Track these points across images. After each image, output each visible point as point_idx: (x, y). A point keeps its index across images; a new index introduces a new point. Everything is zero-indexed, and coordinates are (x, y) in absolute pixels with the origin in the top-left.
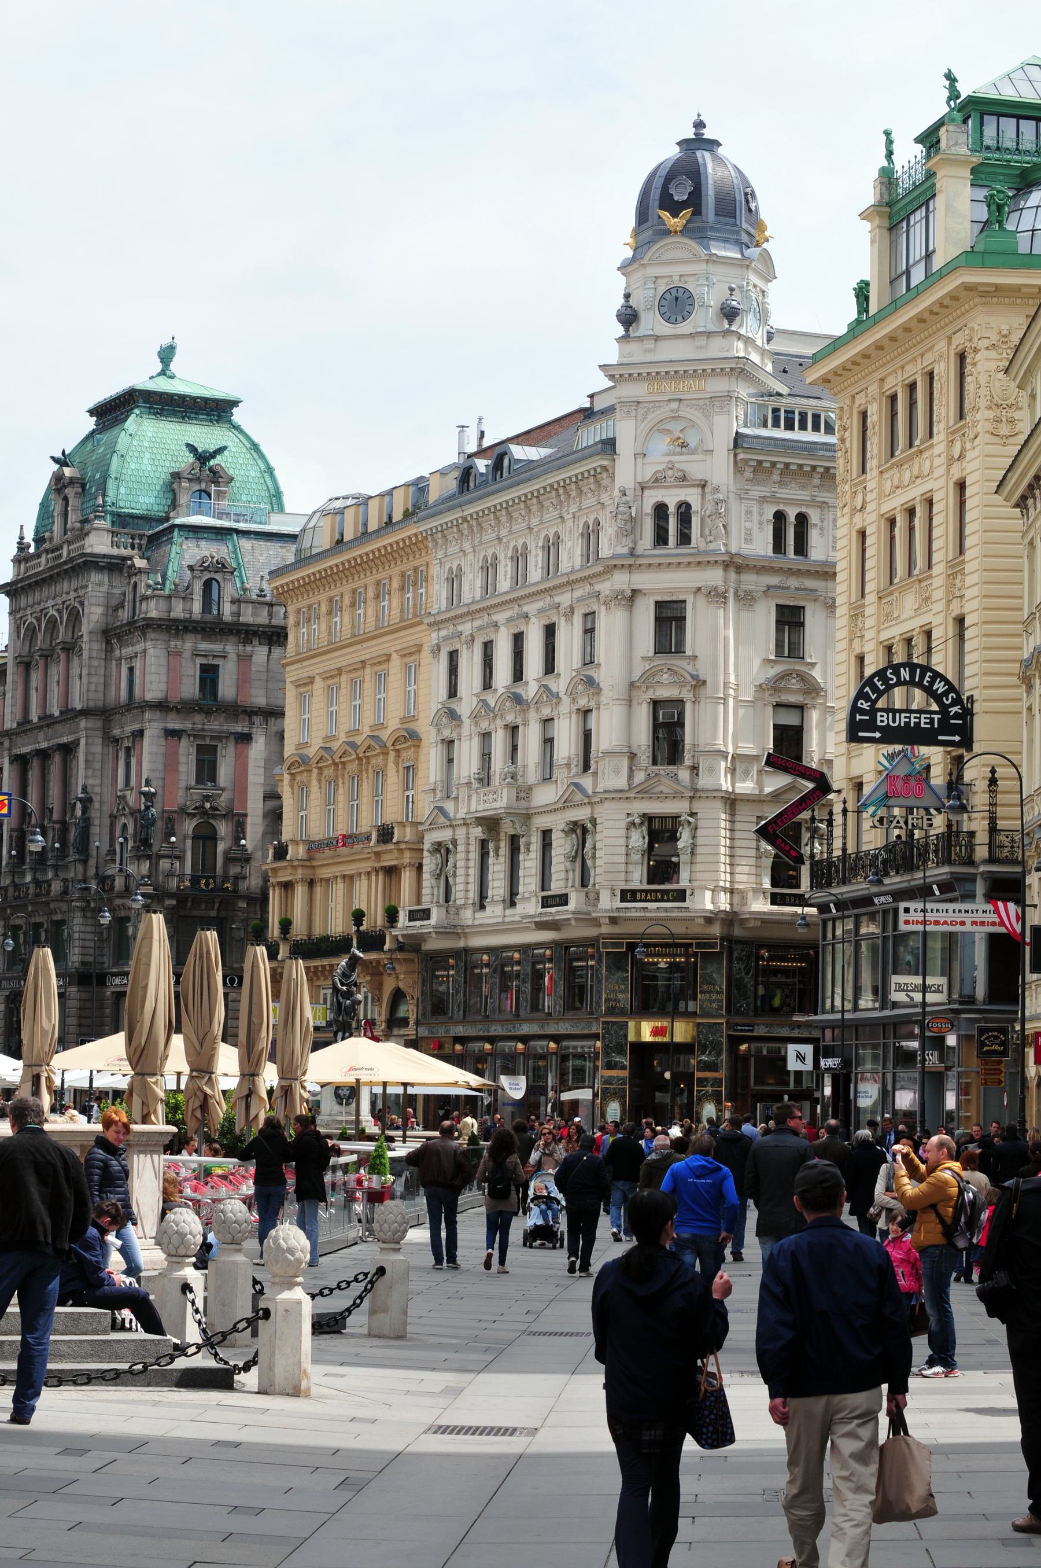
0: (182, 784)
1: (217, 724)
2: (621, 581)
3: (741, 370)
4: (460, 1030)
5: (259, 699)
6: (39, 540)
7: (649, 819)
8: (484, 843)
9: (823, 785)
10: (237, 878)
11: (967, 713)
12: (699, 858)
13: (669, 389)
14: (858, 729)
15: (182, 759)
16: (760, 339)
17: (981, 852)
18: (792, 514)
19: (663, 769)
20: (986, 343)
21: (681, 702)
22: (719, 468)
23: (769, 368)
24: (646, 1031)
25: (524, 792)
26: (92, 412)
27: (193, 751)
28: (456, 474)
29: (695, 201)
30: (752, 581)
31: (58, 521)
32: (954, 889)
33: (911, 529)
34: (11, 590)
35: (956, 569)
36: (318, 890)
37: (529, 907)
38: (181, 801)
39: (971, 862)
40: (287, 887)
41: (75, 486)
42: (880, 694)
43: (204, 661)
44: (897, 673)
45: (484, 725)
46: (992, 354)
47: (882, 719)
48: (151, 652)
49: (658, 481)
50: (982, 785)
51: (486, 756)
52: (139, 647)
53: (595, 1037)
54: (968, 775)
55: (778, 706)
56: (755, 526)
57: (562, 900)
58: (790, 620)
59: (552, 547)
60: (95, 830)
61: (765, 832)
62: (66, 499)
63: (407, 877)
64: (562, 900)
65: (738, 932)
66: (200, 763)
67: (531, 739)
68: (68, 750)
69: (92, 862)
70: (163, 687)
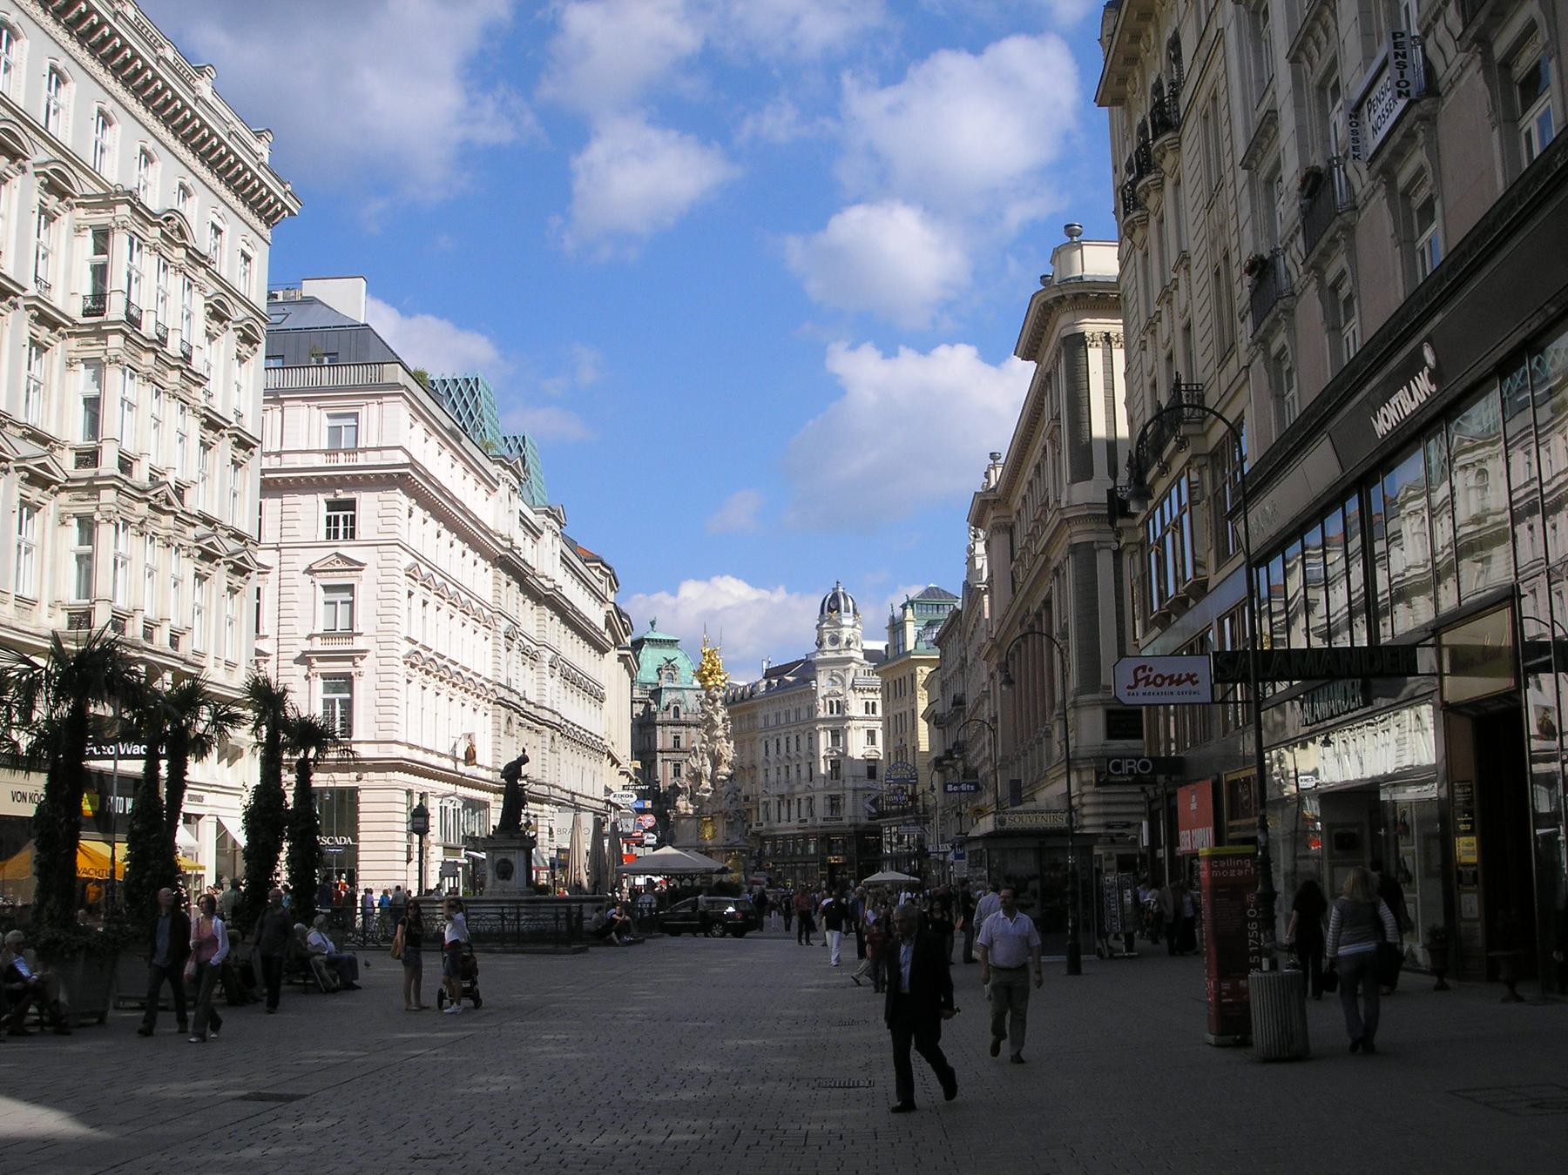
1: (679, 756)
3: (850, 660)
37: (794, 823)
49: (829, 695)
59: (798, 711)
67: (793, 770)
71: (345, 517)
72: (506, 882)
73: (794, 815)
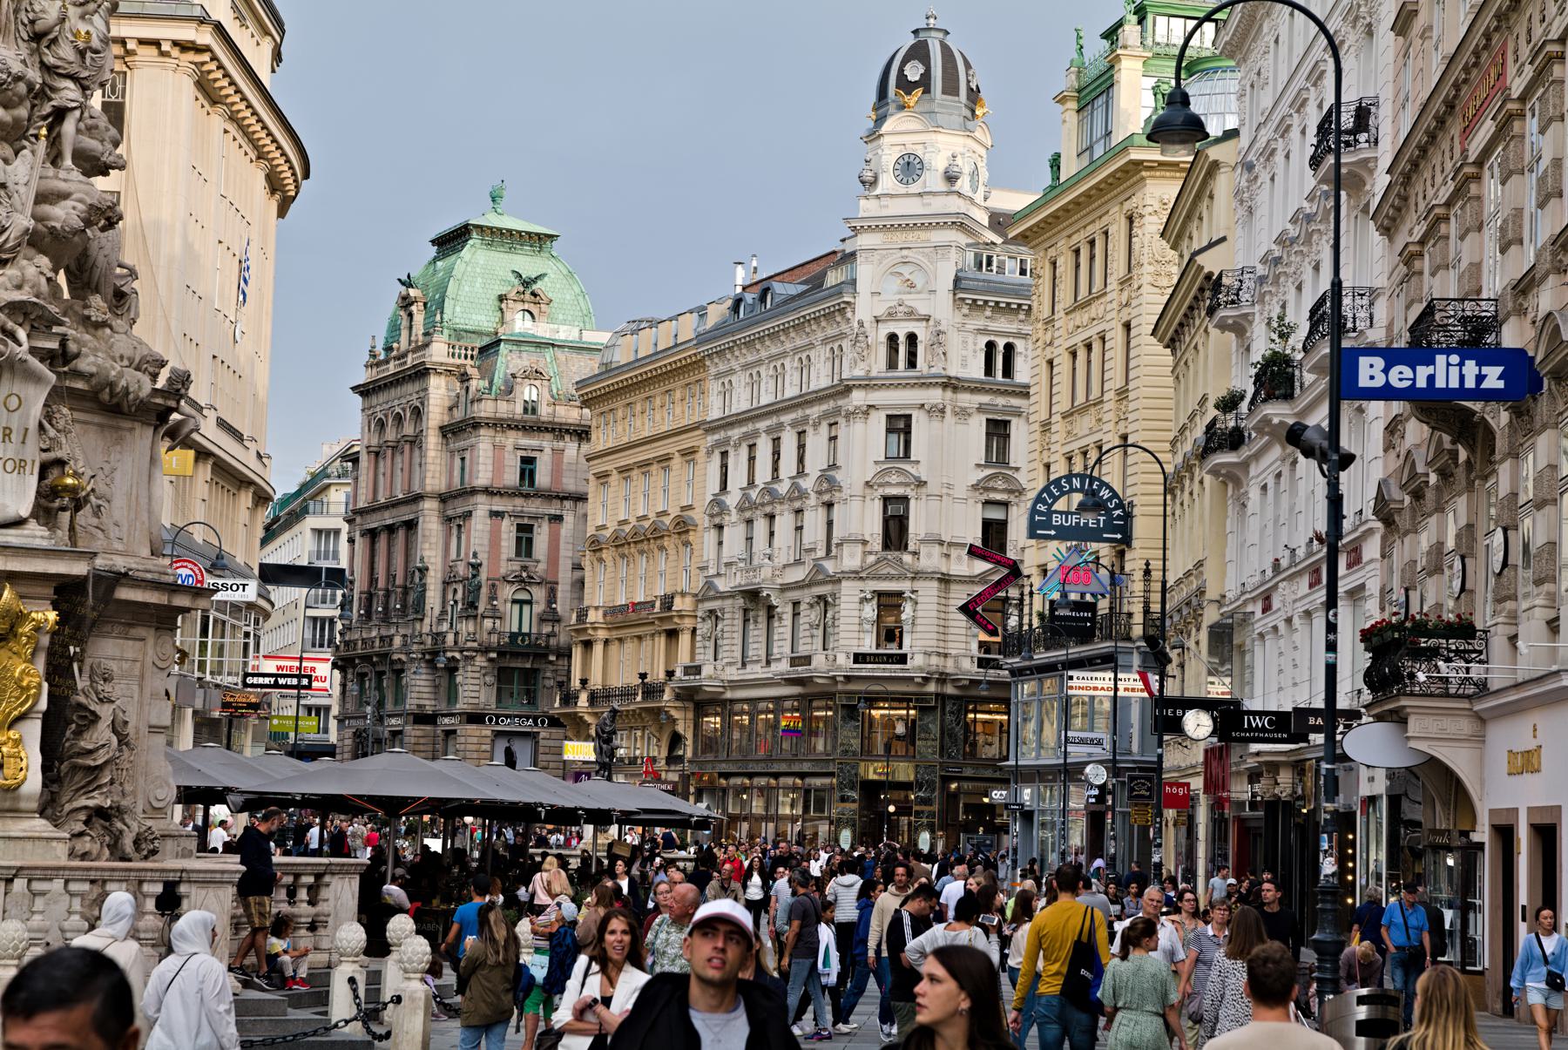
0: (504, 557)
1: (534, 507)
3: (961, 224)
4: (724, 768)
5: (569, 484)
6: (389, 349)
7: (880, 594)
8: (746, 611)
9: (1015, 572)
10: (548, 636)
11: (1128, 517)
12: (919, 628)
13: (899, 238)
14: (1035, 530)
15: (504, 536)
16: (979, 197)
17: (1137, 631)
18: (1001, 343)
19: (891, 555)
20: (1150, 209)
21: (904, 499)
22: (941, 306)
23: (986, 222)
24: (873, 771)
26: (433, 242)
27: (514, 529)
28: (729, 303)
29: (925, 82)
30: (967, 400)
31: (404, 333)
33: (1089, 362)
34: (364, 391)
35: (1122, 393)
36: (614, 648)
38: (503, 571)
39: (1129, 639)
40: (588, 645)
41: (418, 302)
42: (1056, 499)
43: (524, 454)
44: (1070, 483)
45: (748, 514)
46: (1154, 219)
47: (1057, 520)
48: (481, 446)
49: (891, 316)
50: (1138, 575)
51: (749, 539)
52: (467, 443)
53: (832, 775)
54: (1127, 569)
55: (987, 503)
56: (970, 353)
57: (807, 660)
58: (998, 430)
60: (429, 594)
61: (964, 609)
62: (410, 315)
63: (685, 639)
64: (807, 660)
65: (950, 690)
66: (519, 539)
68: (411, 525)
69: (427, 621)
70: (490, 475)
73: (782, 648)
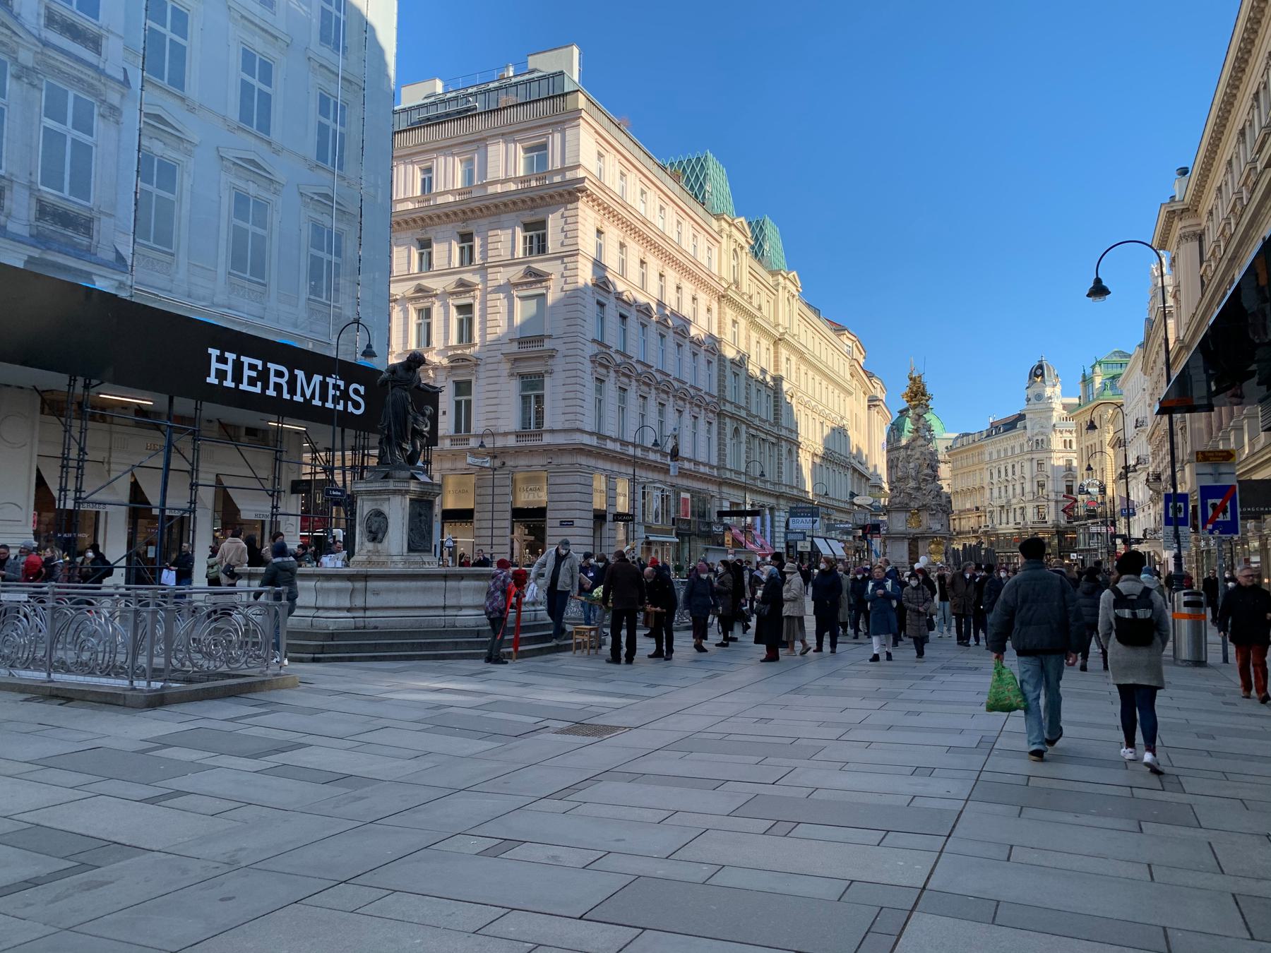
2: (1029, 456)
9: (1076, 501)
25: (1009, 501)
29: (1042, 375)
32: (1104, 523)
37: (1012, 525)
59: (1013, 448)
71: (538, 236)
72: (380, 546)
73: (1011, 519)
